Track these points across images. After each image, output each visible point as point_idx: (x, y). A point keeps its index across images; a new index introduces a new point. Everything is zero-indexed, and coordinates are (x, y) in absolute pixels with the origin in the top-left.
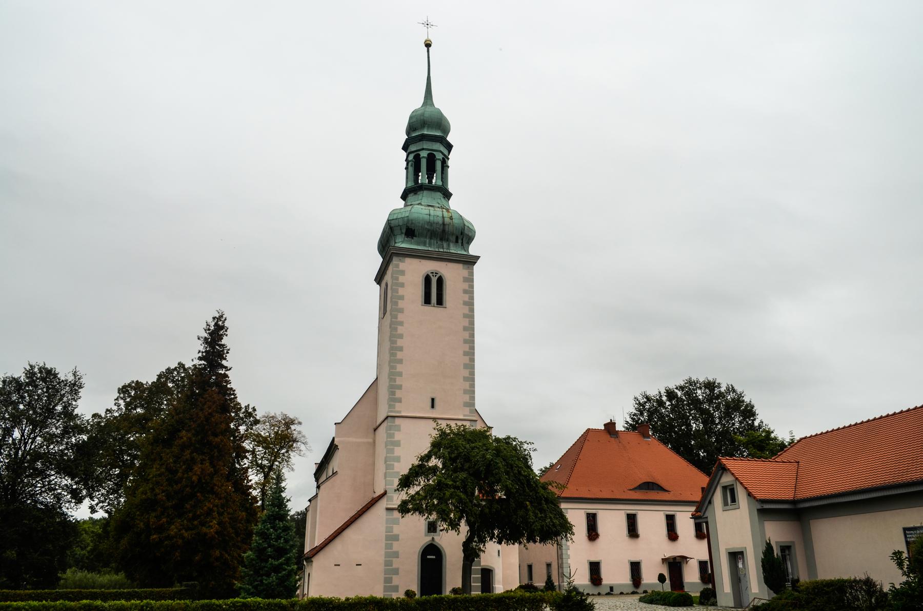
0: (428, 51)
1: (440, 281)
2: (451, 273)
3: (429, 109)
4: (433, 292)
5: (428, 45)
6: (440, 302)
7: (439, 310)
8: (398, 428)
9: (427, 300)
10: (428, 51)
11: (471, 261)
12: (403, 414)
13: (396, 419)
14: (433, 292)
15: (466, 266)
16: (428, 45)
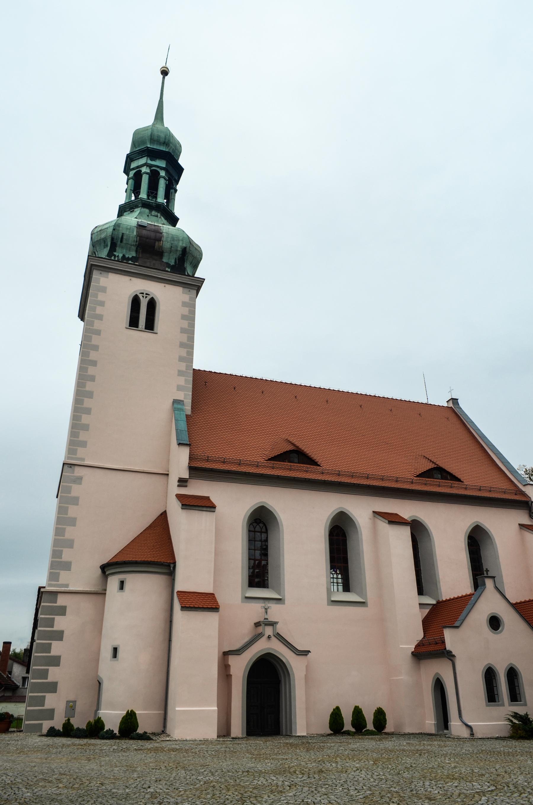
0: (164, 78)
1: (152, 305)
2: (167, 296)
3: (159, 126)
4: (142, 315)
5: (165, 73)
6: (150, 326)
7: (148, 335)
8: (79, 480)
9: (134, 322)
10: (164, 78)
11: (196, 285)
12: (87, 463)
13: (77, 469)
14: (142, 315)
15: (186, 290)
16: (165, 73)
